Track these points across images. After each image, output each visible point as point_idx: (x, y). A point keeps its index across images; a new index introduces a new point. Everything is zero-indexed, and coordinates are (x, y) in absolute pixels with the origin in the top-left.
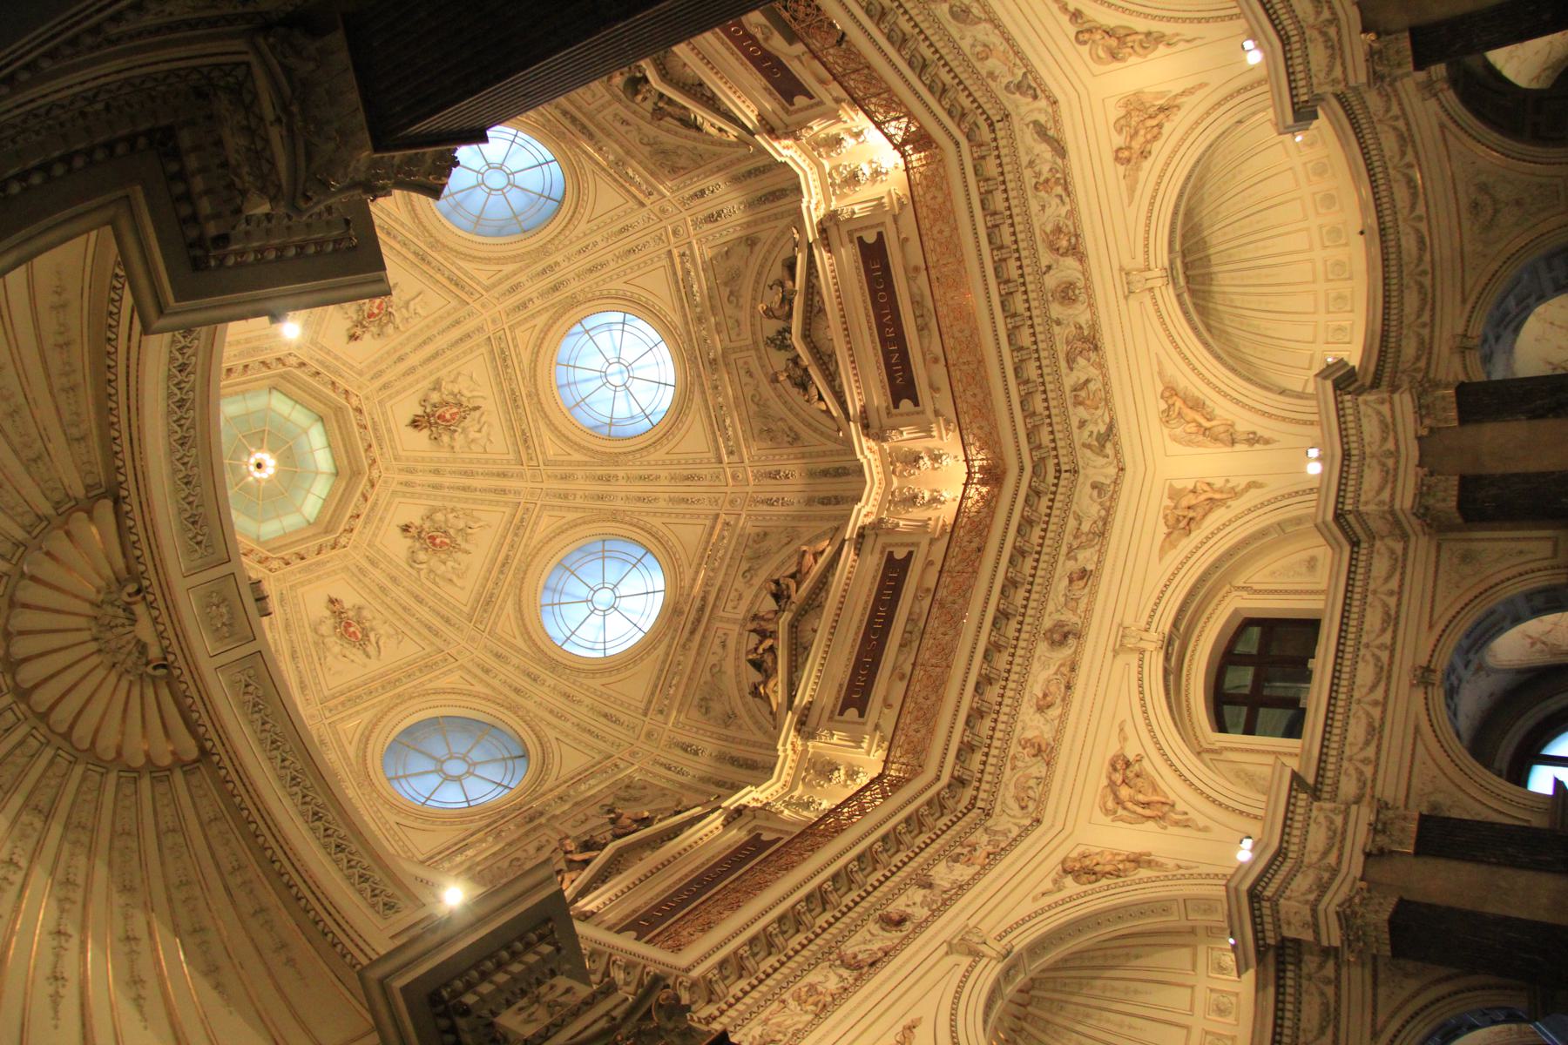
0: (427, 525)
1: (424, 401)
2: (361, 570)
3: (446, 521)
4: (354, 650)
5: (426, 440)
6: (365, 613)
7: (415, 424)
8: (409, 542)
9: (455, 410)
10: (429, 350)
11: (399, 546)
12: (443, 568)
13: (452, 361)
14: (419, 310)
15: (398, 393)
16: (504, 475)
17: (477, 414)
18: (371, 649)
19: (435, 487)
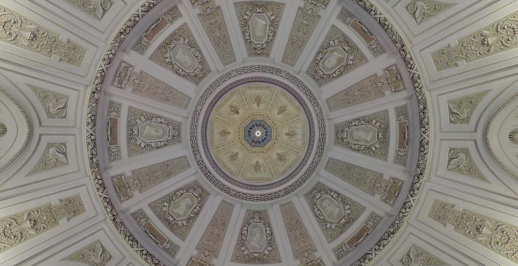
0: (256, 102)
1: (234, 114)
2: (269, 110)
3: (253, 100)
4: (287, 108)
5: (240, 110)
6: (278, 108)
7: (238, 113)
8: (260, 104)
9: (232, 108)
10: (225, 119)
11: (262, 106)
12: (263, 97)
13: (224, 114)
14: (219, 126)
15: (234, 119)
16: (240, 94)
17: (231, 105)
18: (285, 105)
19: (248, 104)
